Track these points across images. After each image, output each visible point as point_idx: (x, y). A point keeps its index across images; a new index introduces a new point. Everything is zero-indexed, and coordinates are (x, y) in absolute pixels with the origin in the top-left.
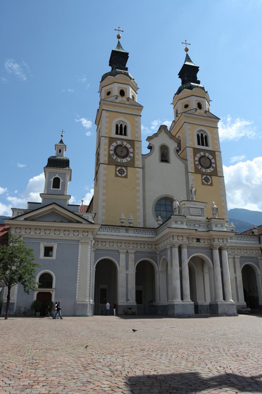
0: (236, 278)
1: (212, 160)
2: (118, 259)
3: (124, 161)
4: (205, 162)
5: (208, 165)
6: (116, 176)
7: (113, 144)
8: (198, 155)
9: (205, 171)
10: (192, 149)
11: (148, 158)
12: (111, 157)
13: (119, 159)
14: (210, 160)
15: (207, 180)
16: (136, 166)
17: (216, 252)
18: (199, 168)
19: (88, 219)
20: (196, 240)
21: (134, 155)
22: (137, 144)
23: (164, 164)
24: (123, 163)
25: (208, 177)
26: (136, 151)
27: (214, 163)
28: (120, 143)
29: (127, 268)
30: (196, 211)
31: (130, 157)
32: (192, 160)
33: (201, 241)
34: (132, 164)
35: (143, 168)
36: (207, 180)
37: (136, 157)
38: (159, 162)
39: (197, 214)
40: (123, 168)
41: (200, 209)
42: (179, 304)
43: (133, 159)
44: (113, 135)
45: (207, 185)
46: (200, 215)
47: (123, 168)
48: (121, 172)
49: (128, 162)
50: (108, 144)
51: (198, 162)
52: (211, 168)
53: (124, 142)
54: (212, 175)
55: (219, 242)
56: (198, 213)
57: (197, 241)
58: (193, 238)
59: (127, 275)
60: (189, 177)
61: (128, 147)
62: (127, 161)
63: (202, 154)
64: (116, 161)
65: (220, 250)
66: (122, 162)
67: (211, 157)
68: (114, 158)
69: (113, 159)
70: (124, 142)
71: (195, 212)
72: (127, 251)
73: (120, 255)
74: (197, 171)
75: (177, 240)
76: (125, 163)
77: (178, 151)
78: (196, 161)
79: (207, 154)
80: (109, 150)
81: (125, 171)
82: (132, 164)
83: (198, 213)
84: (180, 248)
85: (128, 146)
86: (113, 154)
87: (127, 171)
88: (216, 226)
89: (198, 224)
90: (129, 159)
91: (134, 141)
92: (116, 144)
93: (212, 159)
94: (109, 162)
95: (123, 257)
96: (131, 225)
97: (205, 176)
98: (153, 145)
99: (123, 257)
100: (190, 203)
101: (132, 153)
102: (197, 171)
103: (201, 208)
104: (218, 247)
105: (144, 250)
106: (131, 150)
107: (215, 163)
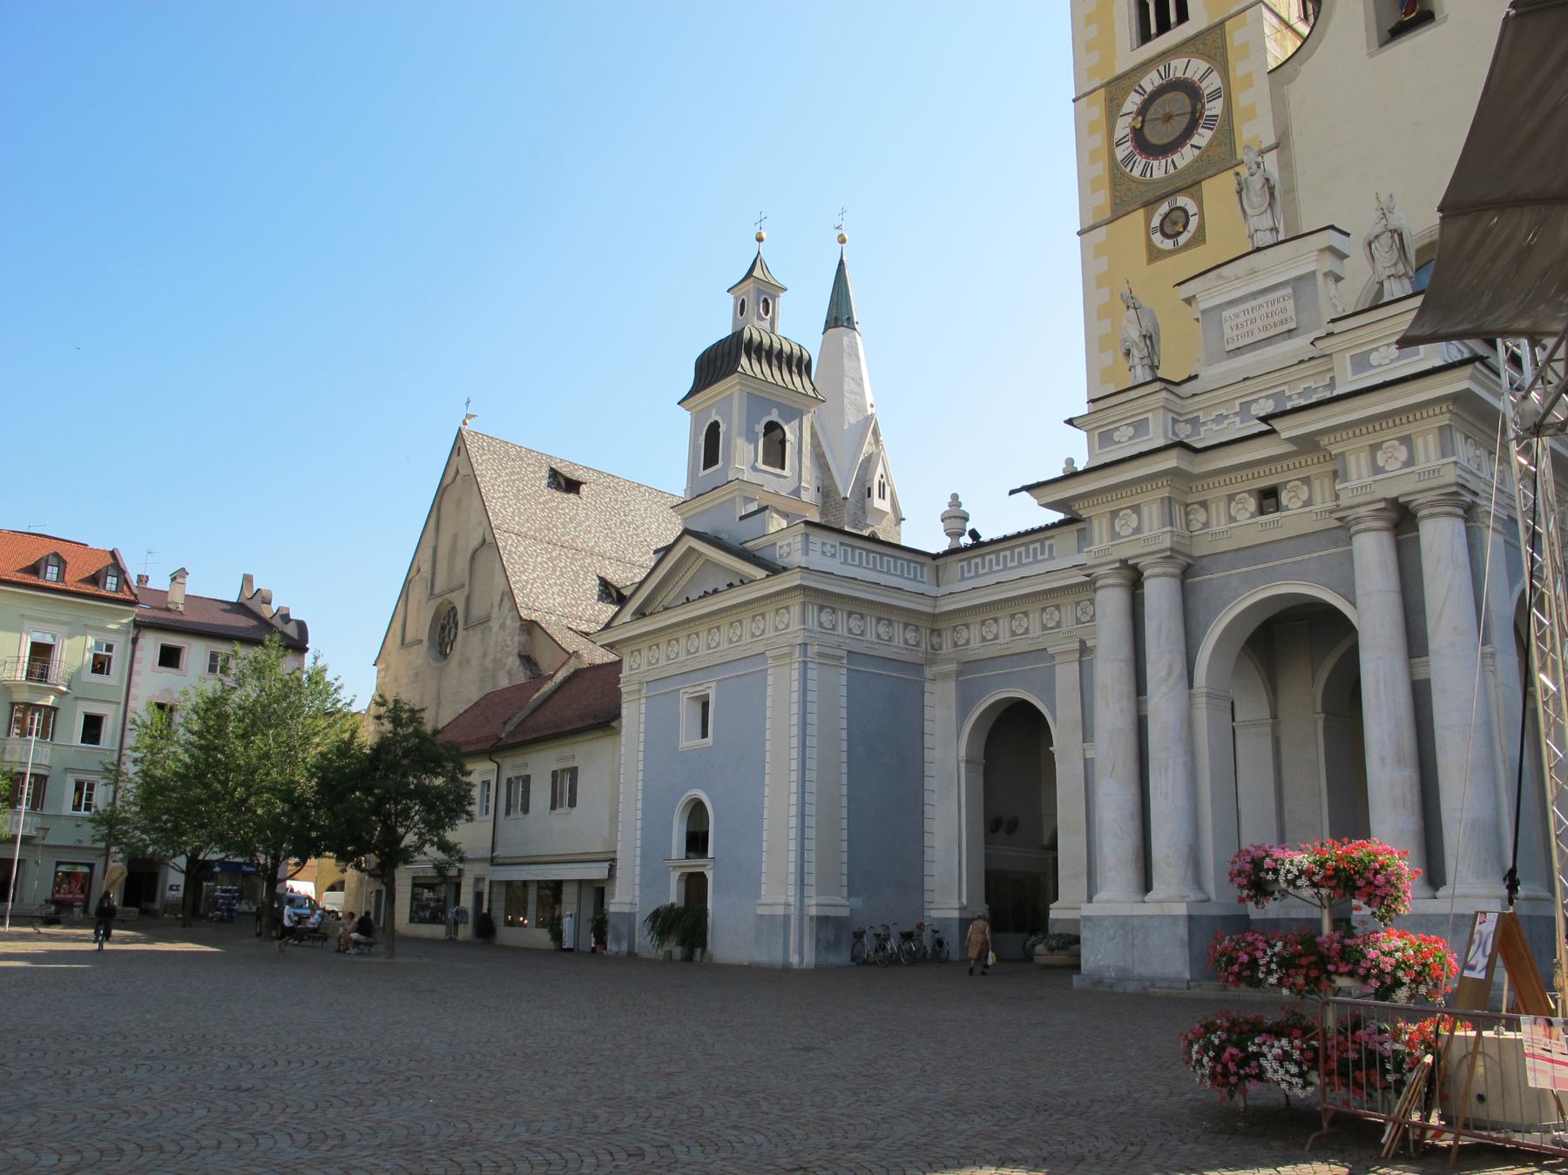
2: (1048, 690)
3: (1181, 164)
6: (1154, 254)
7: (1125, 110)
13: (1156, 163)
17: (1372, 552)
19: (789, 554)
20: (1252, 505)
22: (1235, 36)
24: (1180, 174)
26: (1238, 69)
28: (1158, 82)
29: (1087, 734)
30: (1264, 311)
33: (1284, 498)
34: (1222, 157)
37: (1241, 99)
39: (1265, 328)
40: (1182, 201)
41: (1289, 291)
42: (1101, 918)
43: (1226, 129)
46: (1293, 326)
47: (1182, 201)
48: (1173, 225)
53: (1173, 63)
55: (1377, 470)
56: (1271, 321)
57: (1262, 512)
58: (1231, 498)
59: (1088, 764)
61: (1196, 79)
62: (1197, 152)
65: (1402, 519)
66: (1171, 170)
68: (1136, 173)
69: (1133, 180)
70: (1173, 63)
71: (1253, 321)
72: (1082, 642)
73: (1058, 669)
75: (1106, 544)
80: (1113, 144)
81: (1192, 208)
82: (1222, 157)
83: (1276, 319)
84: (1134, 580)
85: (1193, 68)
86: (1128, 159)
87: (1200, 204)
88: (1361, 363)
89: (1267, 397)
90: (1202, 137)
91: (1221, 24)
95: (1066, 675)
99: (1066, 675)
100: (1220, 277)
101: (1215, 95)
103: (1299, 279)
104: (1362, 511)
106: (1212, 83)
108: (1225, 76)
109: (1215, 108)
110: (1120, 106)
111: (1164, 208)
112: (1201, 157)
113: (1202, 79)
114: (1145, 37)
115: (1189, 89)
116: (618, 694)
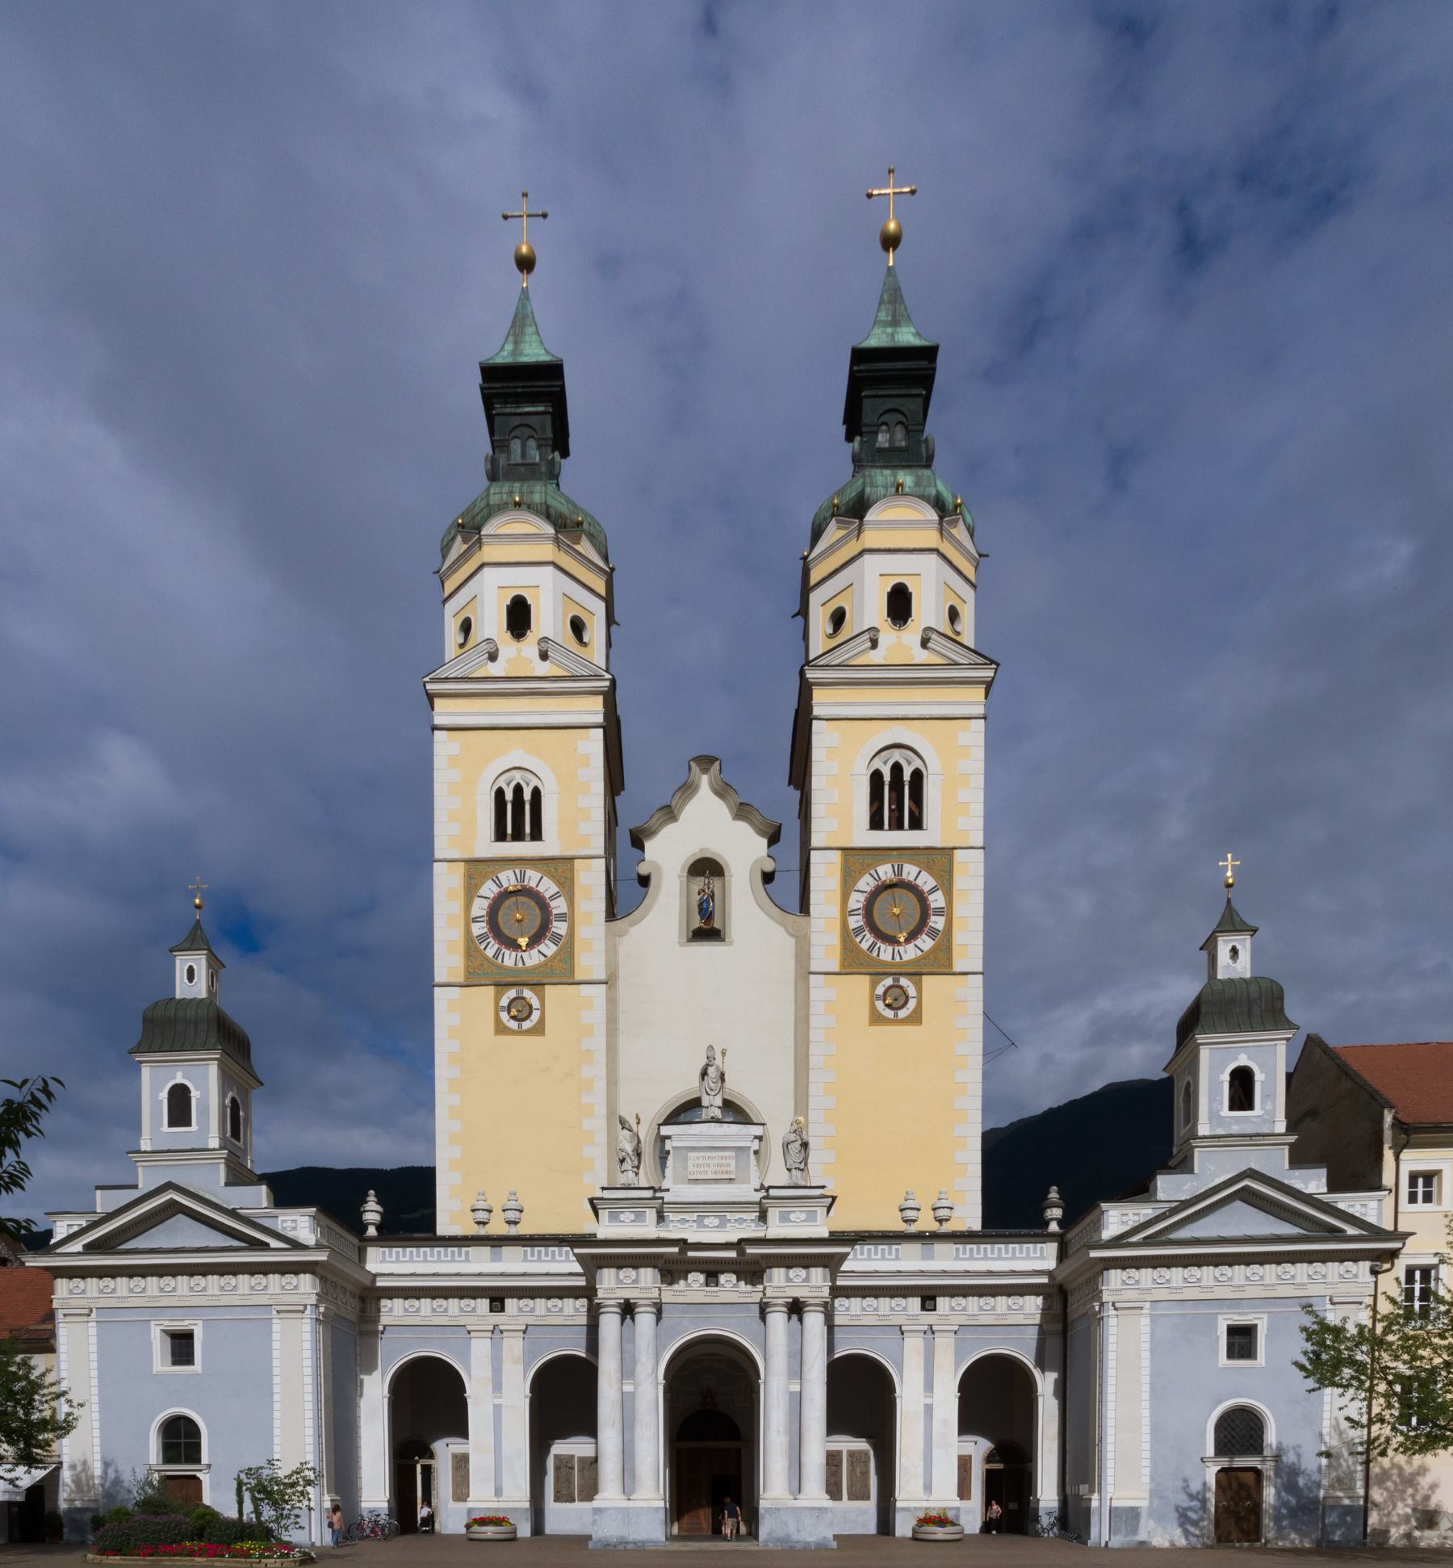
0: (929, 1410)
1: (931, 898)
3: (529, 963)
4: (896, 911)
5: (913, 923)
8: (866, 883)
9: (889, 959)
10: (836, 856)
11: (634, 930)
12: (477, 950)
13: (507, 952)
14: (921, 897)
15: (896, 999)
16: (578, 977)
18: (865, 946)
21: (571, 928)
23: (706, 950)
25: (904, 981)
27: (939, 912)
31: (556, 938)
32: (835, 911)
35: (609, 982)
36: (896, 999)
37: (582, 932)
38: (681, 944)
40: (527, 993)
44: (485, 845)
45: (896, 1021)
47: (527, 993)
49: (549, 962)
50: (461, 893)
51: (860, 918)
52: (924, 936)
53: (529, 873)
54: (921, 974)
60: (814, 994)
61: (547, 895)
62: (543, 959)
63: (885, 872)
64: (497, 966)
66: (520, 965)
67: (926, 881)
70: (529, 873)
74: (853, 961)
76: (535, 968)
77: (768, 878)
78: (852, 913)
79: (910, 872)
80: (470, 920)
85: (548, 888)
91: (571, 859)
92: (496, 890)
93: (933, 890)
94: (468, 972)
96: (514, 1231)
97: (889, 981)
98: (656, 865)
101: (562, 917)
102: (853, 961)
105: (559, 1321)
106: (559, 906)
107: (947, 912)
108: (571, 904)
109: (560, 928)
110: (477, 887)
111: (512, 993)
112: (544, 964)
113: (553, 897)
114: (500, 836)
115: (543, 904)
116: (50, 1316)
